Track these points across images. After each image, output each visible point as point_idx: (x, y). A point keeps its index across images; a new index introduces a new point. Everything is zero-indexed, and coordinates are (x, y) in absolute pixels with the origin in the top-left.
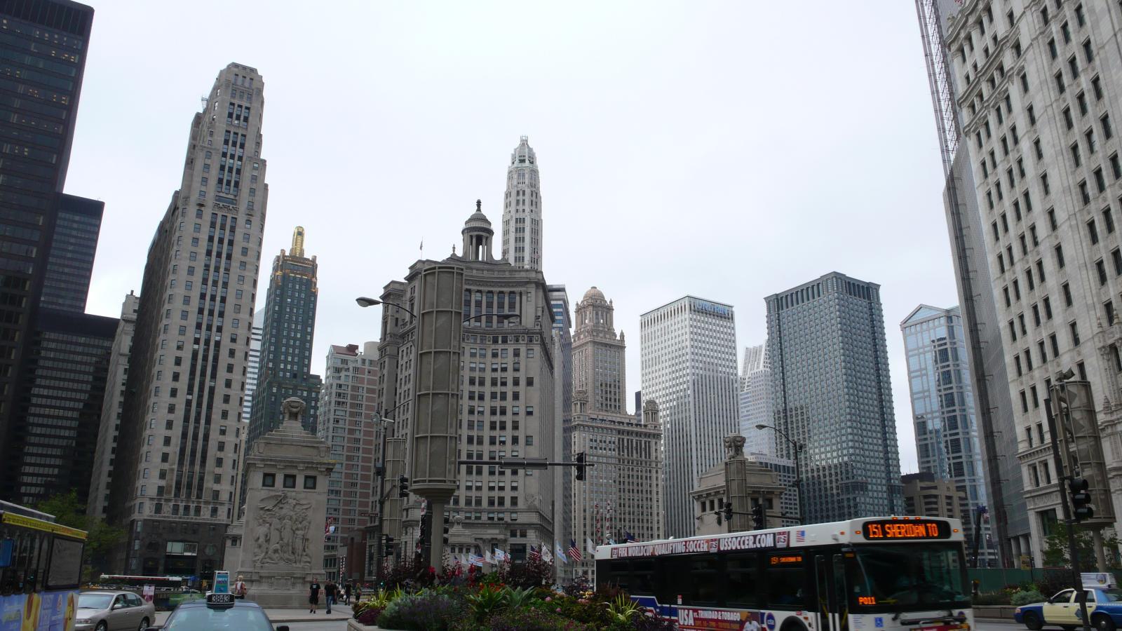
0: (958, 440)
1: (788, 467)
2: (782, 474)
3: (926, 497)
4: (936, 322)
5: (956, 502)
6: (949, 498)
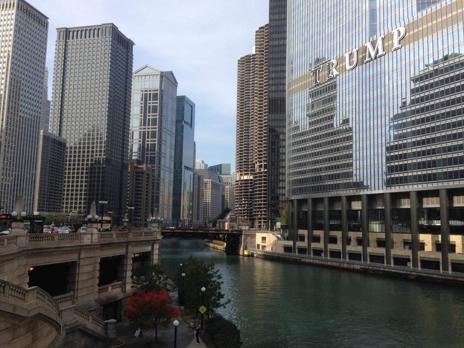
1: (62, 142)
2: (57, 146)
3: (137, 173)
4: (155, 77)
5: (151, 177)
6: (148, 174)
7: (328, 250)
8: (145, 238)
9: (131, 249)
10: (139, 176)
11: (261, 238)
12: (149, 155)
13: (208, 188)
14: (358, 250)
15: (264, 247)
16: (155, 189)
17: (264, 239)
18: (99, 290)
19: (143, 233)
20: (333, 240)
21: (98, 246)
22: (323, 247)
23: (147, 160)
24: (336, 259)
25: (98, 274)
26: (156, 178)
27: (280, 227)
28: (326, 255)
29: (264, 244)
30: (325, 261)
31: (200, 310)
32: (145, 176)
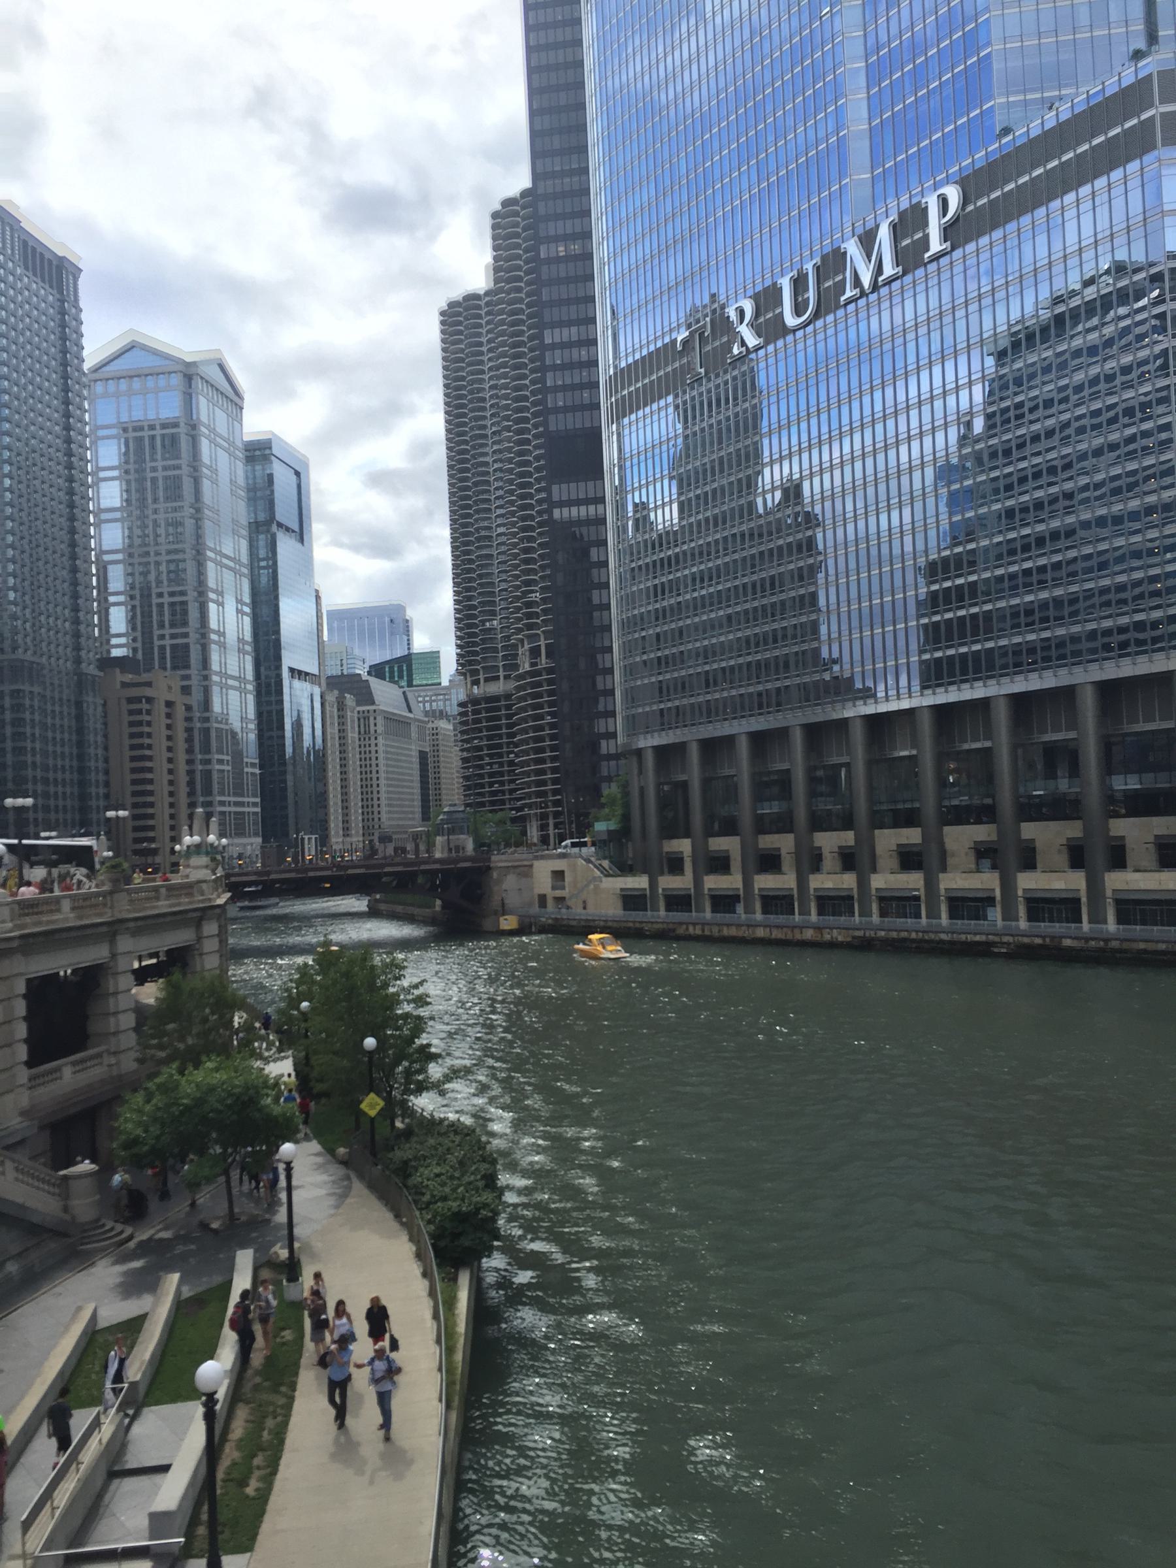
0: (184, 603)
3: (130, 700)
4: (162, 381)
5: (180, 712)
6: (169, 704)
7: (756, 891)
8: (171, 906)
9: (125, 943)
10: (140, 712)
11: (549, 874)
12: (168, 642)
13: (372, 731)
14: (845, 886)
15: (560, 900)
16: (197, 748)
17: (559, 875)
18: (30, 1080)
19: (163, 891)
20: (770, 862)
21: (15, 944)
22: (740, 885)
23: (163, 658)
24: (781, 919)
25: (21, 1030)
26: (197, 715)
27: (605, 837)
28: (749, 910)
29: (558, 893)
30: (749, 926)
31: (363, 1106)
32: (160, 709)
